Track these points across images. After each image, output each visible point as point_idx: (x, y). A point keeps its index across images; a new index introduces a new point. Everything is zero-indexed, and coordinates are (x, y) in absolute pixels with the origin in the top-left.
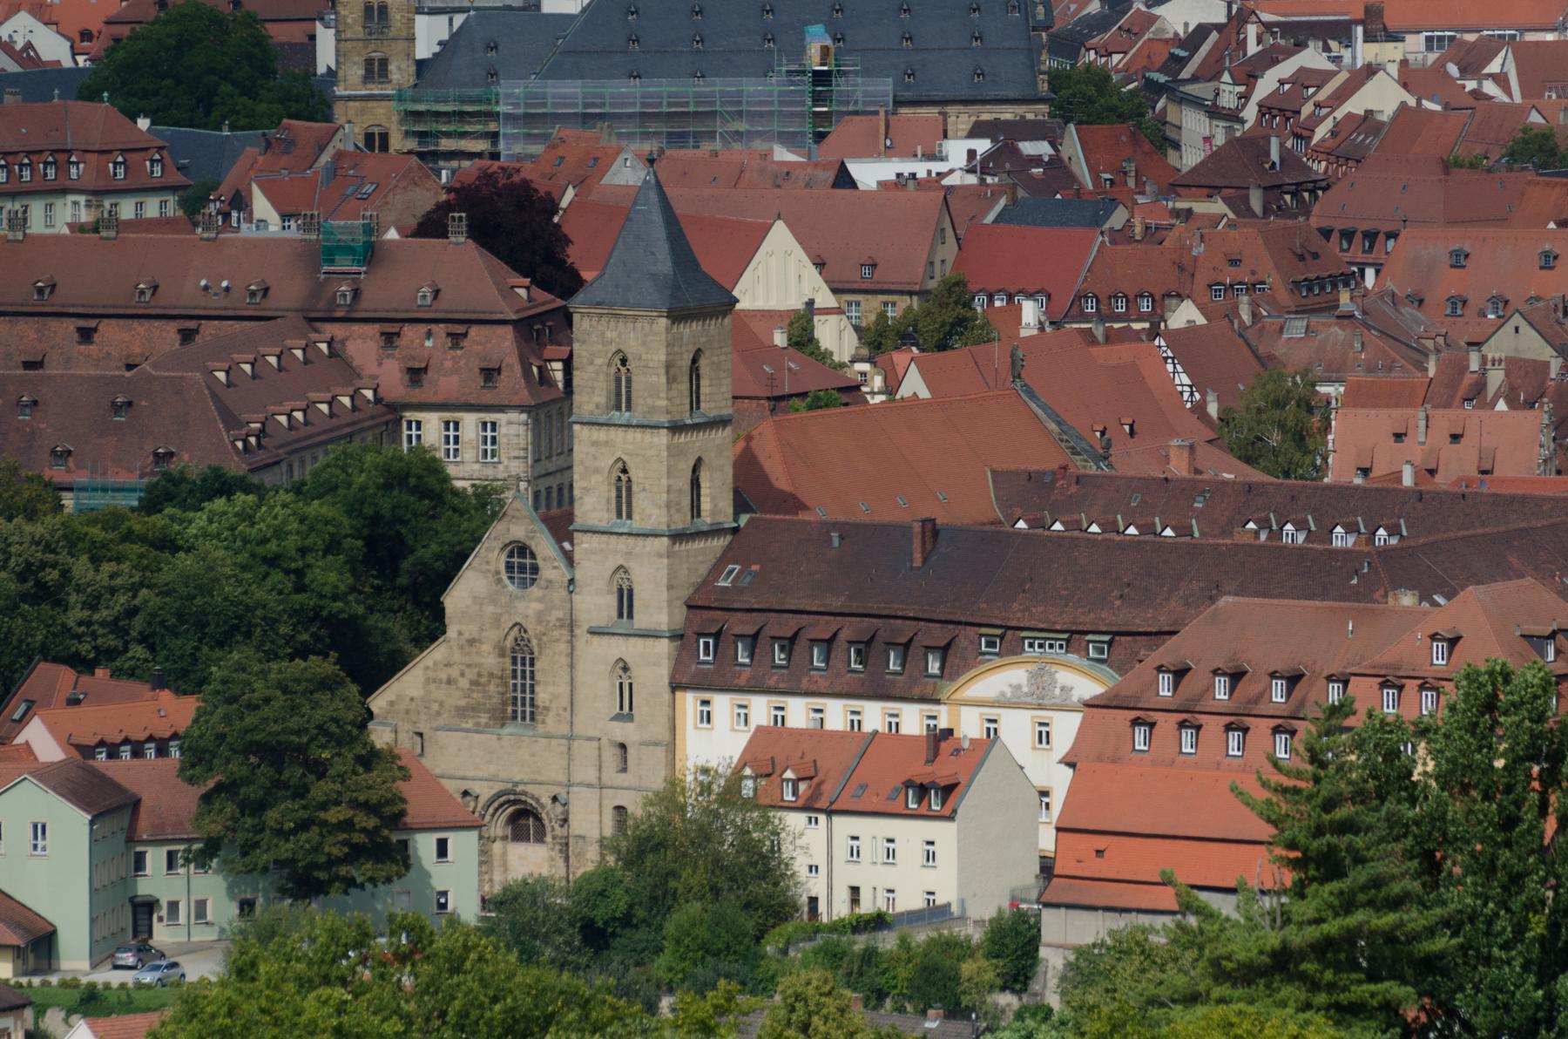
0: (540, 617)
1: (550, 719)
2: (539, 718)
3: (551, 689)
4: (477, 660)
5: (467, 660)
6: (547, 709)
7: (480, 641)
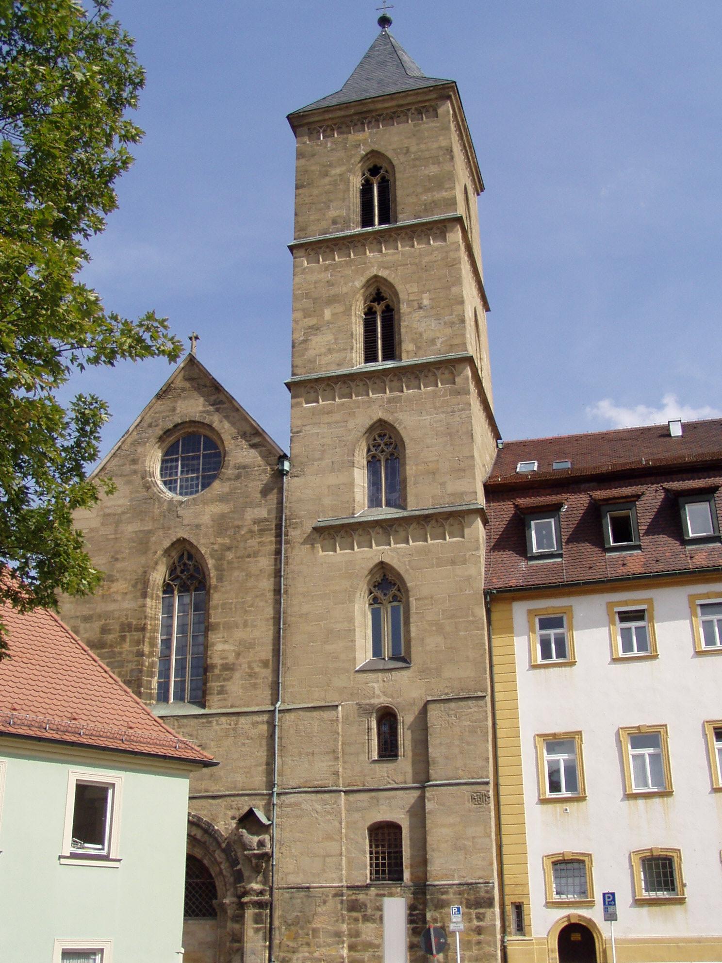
0: (221, 524)
1: (236, 686)
2: (213, 685)
3: (239, 634)
4: (102, 607)
5: (85, 610)
6: (227, 667)
7: (111, 579)
